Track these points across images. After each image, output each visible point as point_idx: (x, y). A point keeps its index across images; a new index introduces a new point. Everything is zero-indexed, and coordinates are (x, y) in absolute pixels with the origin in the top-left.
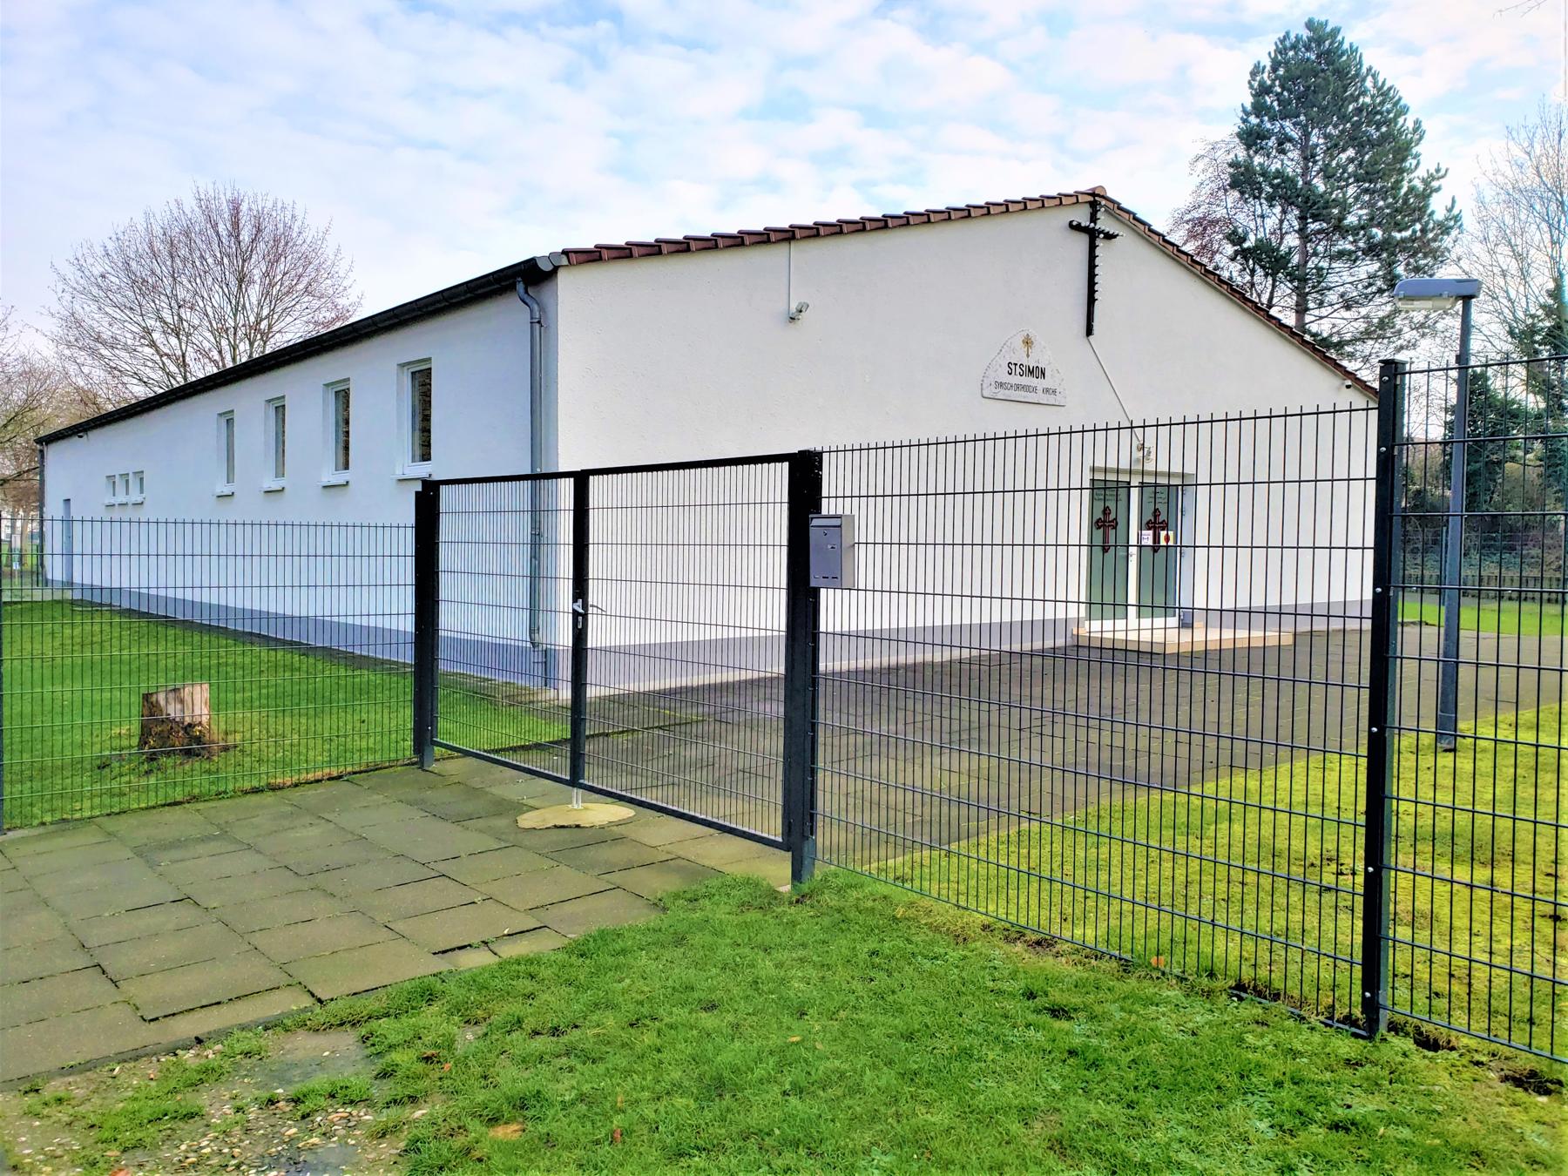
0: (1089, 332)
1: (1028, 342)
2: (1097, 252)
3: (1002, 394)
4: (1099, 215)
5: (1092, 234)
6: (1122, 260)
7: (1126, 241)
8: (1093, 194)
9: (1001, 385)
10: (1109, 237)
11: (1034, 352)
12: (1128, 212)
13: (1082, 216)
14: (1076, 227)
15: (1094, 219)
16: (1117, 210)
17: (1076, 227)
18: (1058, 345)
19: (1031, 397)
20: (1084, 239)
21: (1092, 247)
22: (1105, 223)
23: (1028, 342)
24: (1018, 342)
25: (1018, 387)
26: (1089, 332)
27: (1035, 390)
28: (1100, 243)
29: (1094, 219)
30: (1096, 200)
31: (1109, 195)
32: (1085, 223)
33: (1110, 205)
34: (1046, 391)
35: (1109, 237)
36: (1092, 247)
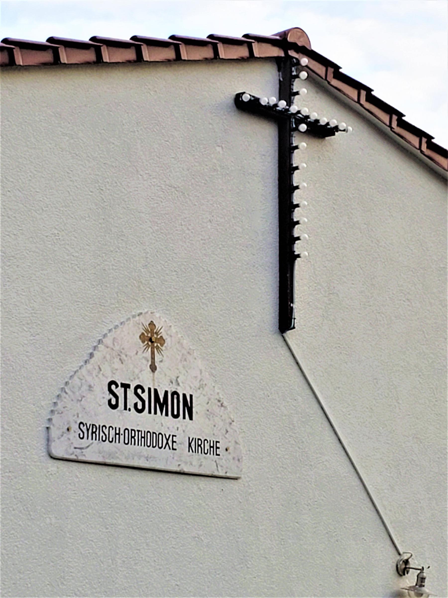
0: (285, 321)
1: (152, 339)
2: (297, 159)
3: (94, 450)
4: (297, 86)
5: (284, 124)
6: (340, 171)
7: (352, 138)
8: (281, 41)
9: (94, 431)
10: (320, 131)
11: (166, 358)
12: (358, 86)
13: (261, 85)
14: (248, 107)
15: (286, 93)
16: (331, 77)
17: (248, 107)
18: (216, 347)
19: (161, 458)
20: (262, 138)
21: (285, 152)
22: (308, 103)
23: (152, 339)
24: (130, 337)
25: (132, 436)
26: (285, 321)
27: (169, 442)
28: (304, 151)
29: (286, 93)
30: (288, 54)
31: (315, 47)
32: (268, 97)
33: (320, 69)
34: (196, 445)
35: (320, 131)
36: (285, 152)
